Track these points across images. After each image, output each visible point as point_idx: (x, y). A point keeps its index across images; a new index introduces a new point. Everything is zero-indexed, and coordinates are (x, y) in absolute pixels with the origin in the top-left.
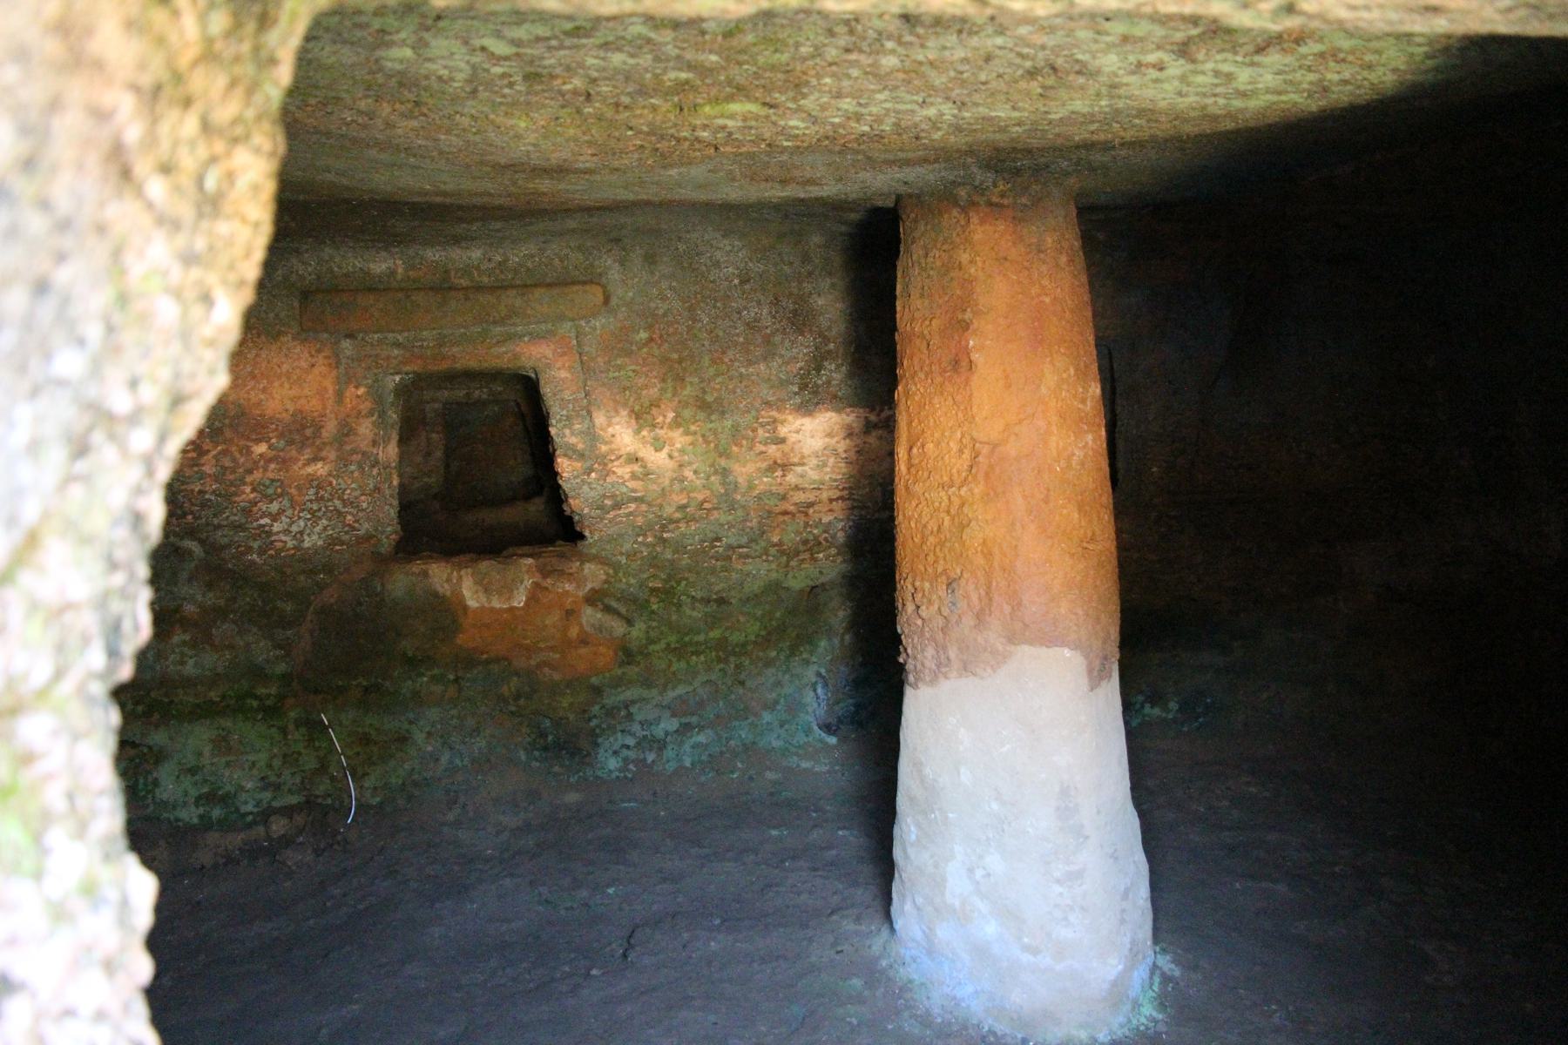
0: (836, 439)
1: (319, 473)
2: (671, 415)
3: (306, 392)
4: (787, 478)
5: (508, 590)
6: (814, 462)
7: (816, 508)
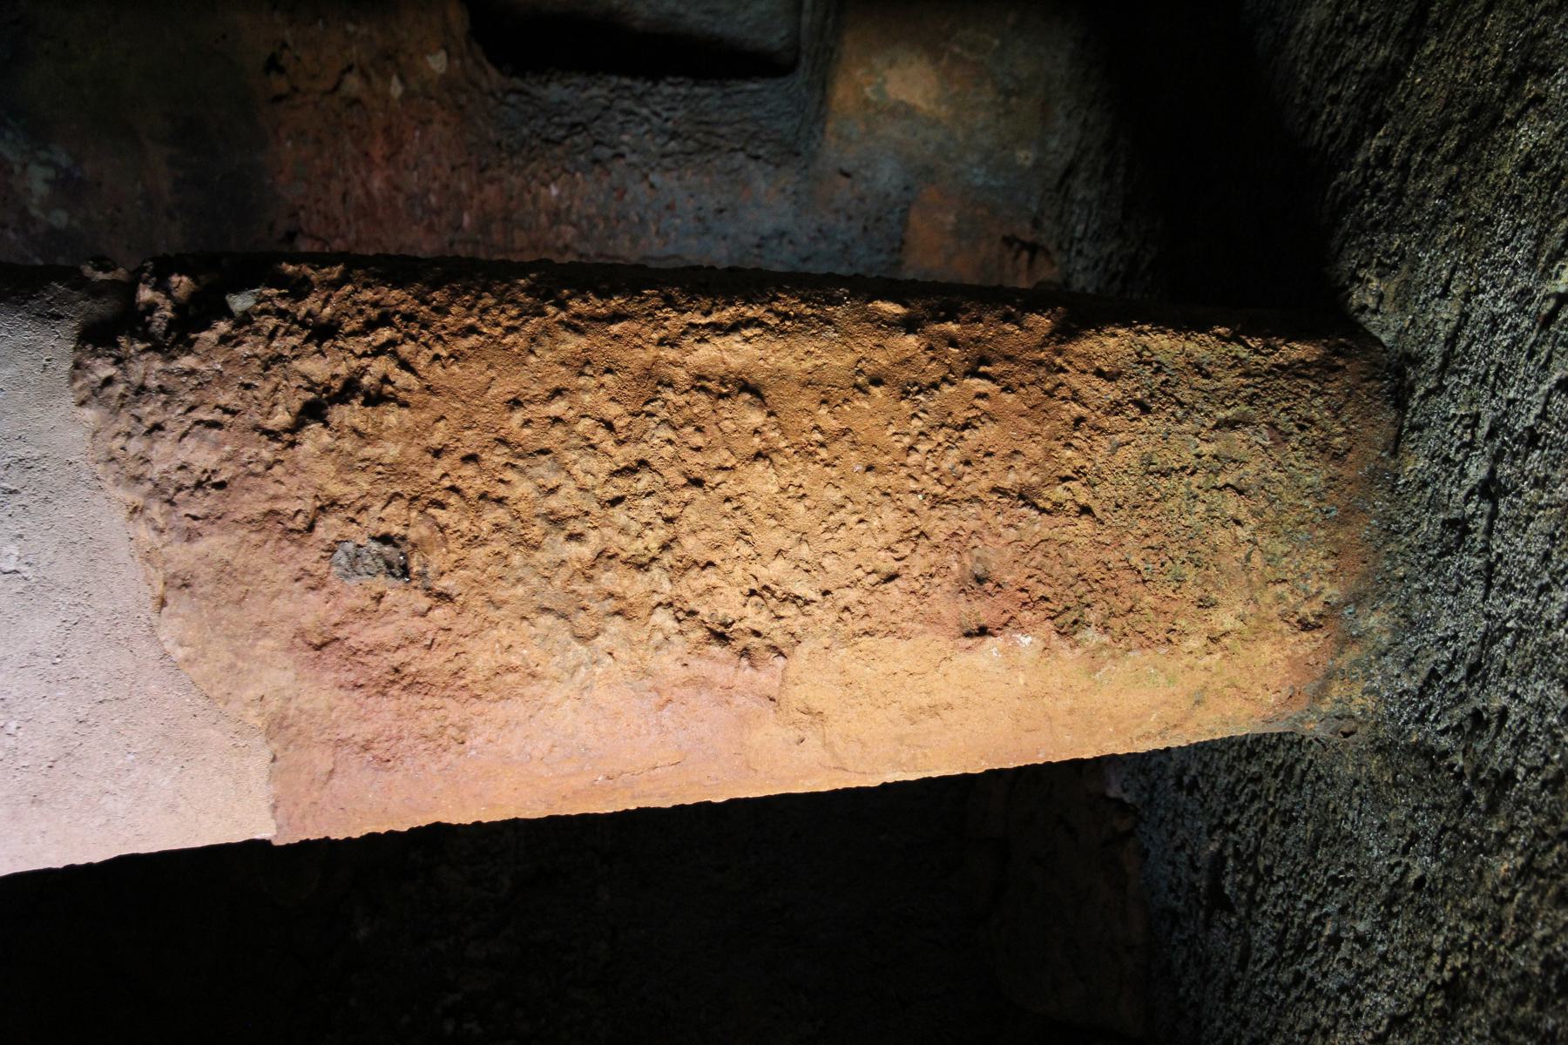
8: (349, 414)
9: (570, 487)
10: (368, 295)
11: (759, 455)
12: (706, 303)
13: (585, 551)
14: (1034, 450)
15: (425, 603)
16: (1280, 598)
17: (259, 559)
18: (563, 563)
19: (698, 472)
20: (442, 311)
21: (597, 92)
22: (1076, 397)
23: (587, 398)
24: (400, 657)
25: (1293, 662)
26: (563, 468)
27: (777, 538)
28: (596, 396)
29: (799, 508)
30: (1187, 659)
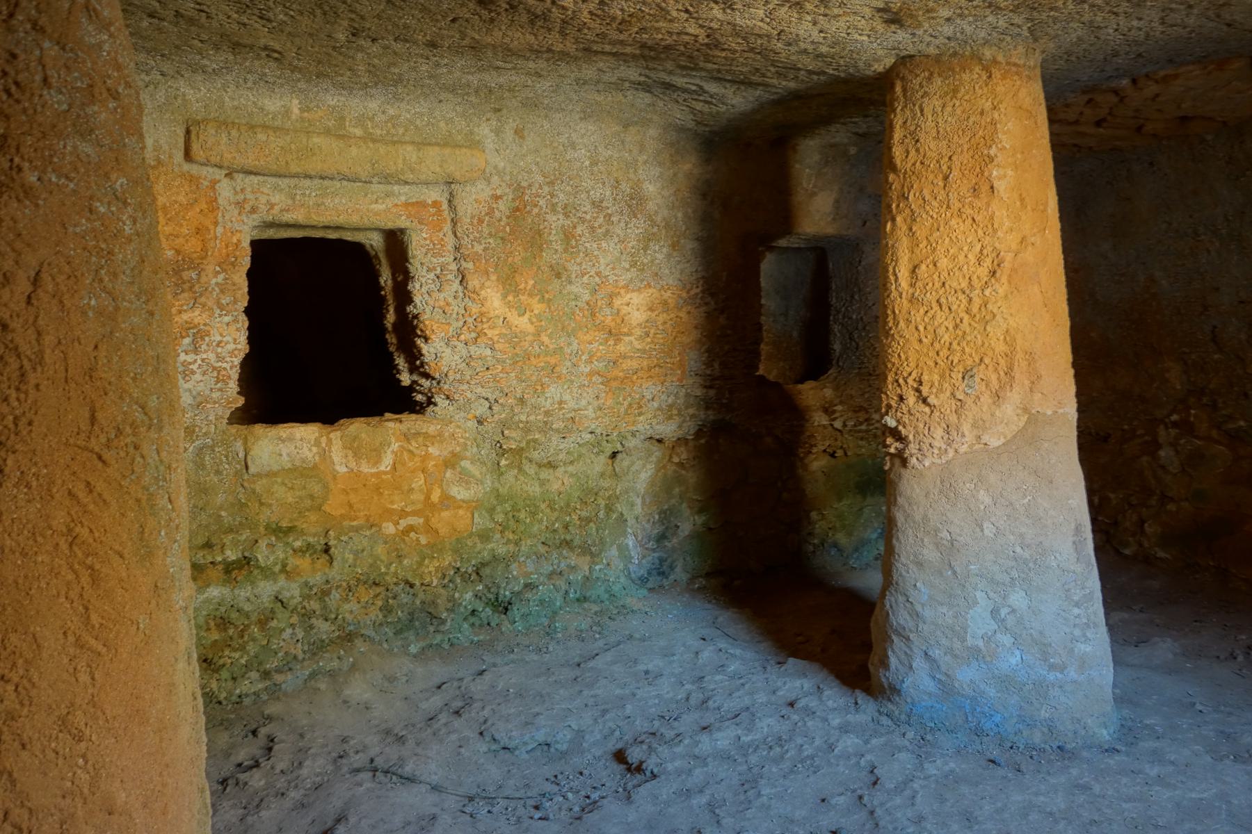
0: (656, 312)
1: (196, 321)
2: (531, 282)
3: (185, 231)
4: (618, 347)
5: (376, 454)
6: (638, 332)
7: (639, 374)
8: (925, 390)
9: (946, 323)
10: (890, 386)
11: (935, 265)
12: (889, 285)
13: (966, 317)
14: (931, 177)
15: (983, 366)
16: (981, 88)
17: (970, 415)
18: (970, 325)
19: (941, 284)
20: (894, 364)
21: (836, 328)
22: (914, 164)
23: (918, 319)
24: (1002, 373)
25: (1004, 78)
26: (940, 325)
27: (961, 257)
28: (917, 316)
29: (952, 251)
30: (1002, 116)
